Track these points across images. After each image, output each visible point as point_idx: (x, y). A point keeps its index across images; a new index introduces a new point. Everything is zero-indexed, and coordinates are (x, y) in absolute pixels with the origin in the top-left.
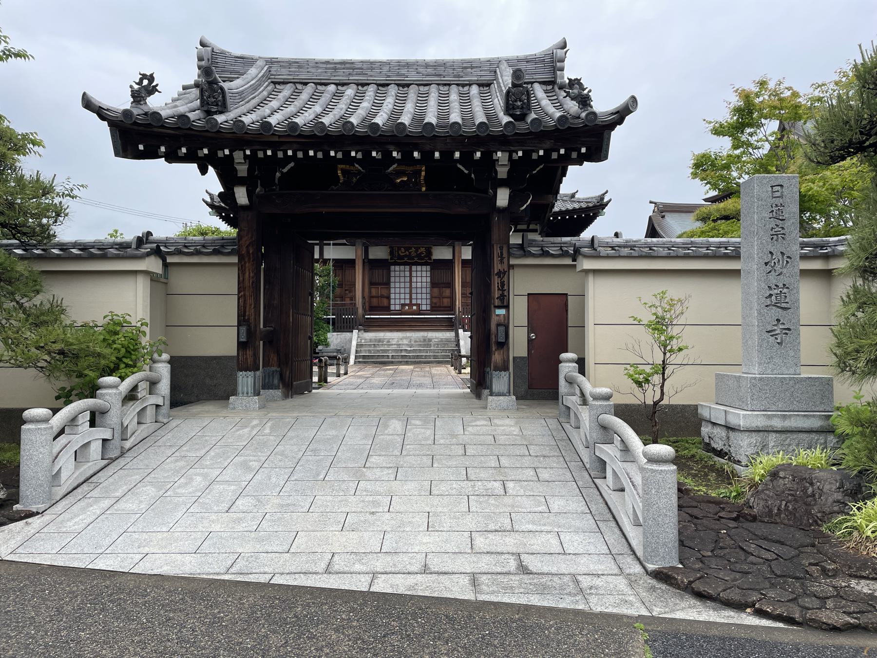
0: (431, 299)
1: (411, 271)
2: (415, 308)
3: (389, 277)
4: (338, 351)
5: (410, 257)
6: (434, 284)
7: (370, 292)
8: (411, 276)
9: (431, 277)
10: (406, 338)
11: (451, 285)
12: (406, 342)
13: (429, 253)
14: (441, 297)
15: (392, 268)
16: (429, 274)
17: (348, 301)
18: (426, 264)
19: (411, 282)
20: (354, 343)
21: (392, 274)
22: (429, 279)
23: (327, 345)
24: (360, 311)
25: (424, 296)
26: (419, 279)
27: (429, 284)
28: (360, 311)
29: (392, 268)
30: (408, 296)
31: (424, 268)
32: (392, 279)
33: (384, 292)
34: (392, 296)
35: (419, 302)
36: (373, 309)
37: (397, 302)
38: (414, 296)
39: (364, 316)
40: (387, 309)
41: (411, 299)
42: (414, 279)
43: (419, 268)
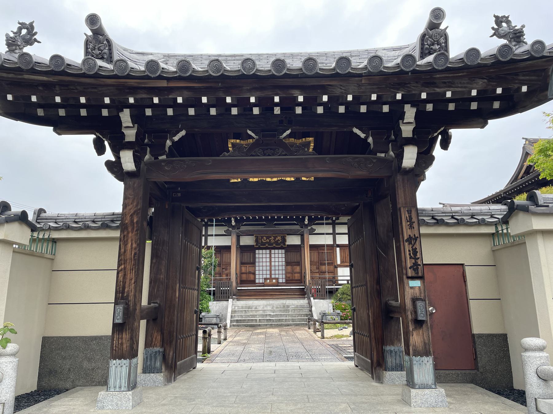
0: (286, 273)
1: (270, 254)
2: (274, 281)
3: (254, 258)
4: (217, 317)
5: (270, 243)
6: (288, 263)
7: (241, 270)
8: (270, 258)
9: (285, 258)
10: (269, 305)
11: (300, 263)
12: (269, 308)
13: (284, 240)
14: (293, 273)
15: (257, 251)
17: (224, 277)
18: (281, 248)
19: (271, 262)
20: (230, 310)
21: (257, 256)
23: (208, 312)
24: (234, 284)
25: (280, 272)
26: (277, 260)
27: (284, 263)
29: (257, 251)
30: (268, 272)
31: (280, 251)
32: (257, 260)
33: (251, 269)
34: (257, 272)
35: (277, 276)
36: (242, 282)
37: (261, 276)
38: (273, 272)
39: (236, 288)
40: (253, 282)
41: (271, 274)
42: (273, 260)
43: (276, 251)
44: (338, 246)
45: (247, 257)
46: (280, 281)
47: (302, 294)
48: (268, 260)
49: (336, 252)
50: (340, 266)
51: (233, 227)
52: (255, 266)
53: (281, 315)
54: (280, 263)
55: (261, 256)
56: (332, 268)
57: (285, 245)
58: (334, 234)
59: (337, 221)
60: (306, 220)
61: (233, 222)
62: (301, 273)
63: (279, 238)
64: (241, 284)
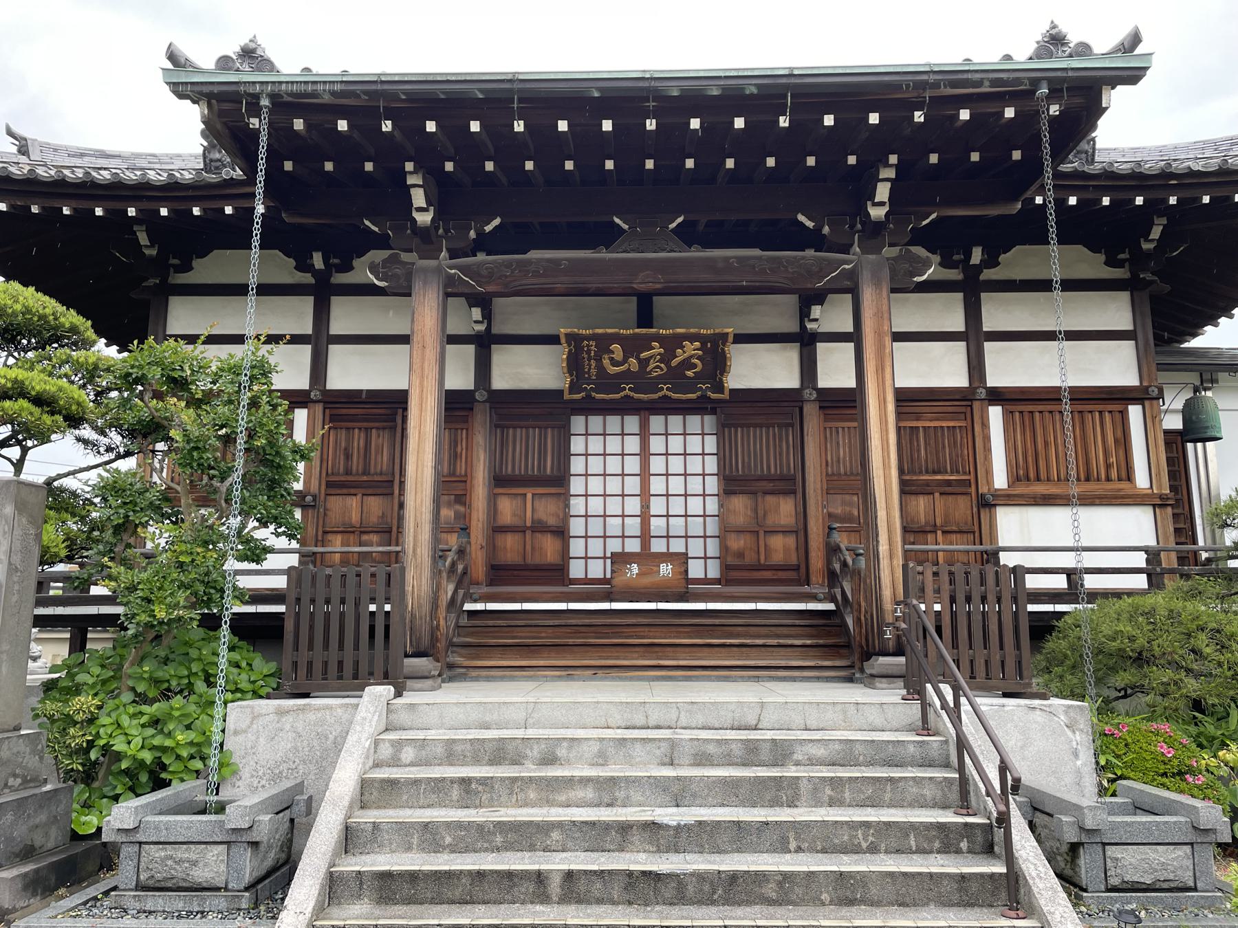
2: (666, 569)
3: (564, 455)
6: (732, 482)
7: (493, 510)
9: (721, 455)
13: (717, 363)
14: (759, 529)
15: (577, 423)
16: (711, 444)
19: (645, 475)
21: (577, 445)
22: (712, 465)
27: (712, 485)
28: (418, 578)
29: (577, 423)
31: (694, 421)
32: (577, 465)
33: (546, 510)
34: (576, 527)
35: (677, 546)
36: (503, 575)
37: (596, 547)
40: (554, 575)
42: (657, 465)
44: (997, 396)
45: (526, 446)
46: (696, 570)
47: (842, 644)
48: (633, 465)
49: (985, 425)
50: (1009, 499)
51: (426, 240)
52: (565, 496)
53: (742, 836)
54: (695, 485)
55: (595, 465)
56: (962, 507)
57: (719, 387)
58: (974, 337)
59: (988, 274)
60: (883, 192)
61: (418, 198)
62: (801, 531)
63: (691, 349)
64: (491, 583)
